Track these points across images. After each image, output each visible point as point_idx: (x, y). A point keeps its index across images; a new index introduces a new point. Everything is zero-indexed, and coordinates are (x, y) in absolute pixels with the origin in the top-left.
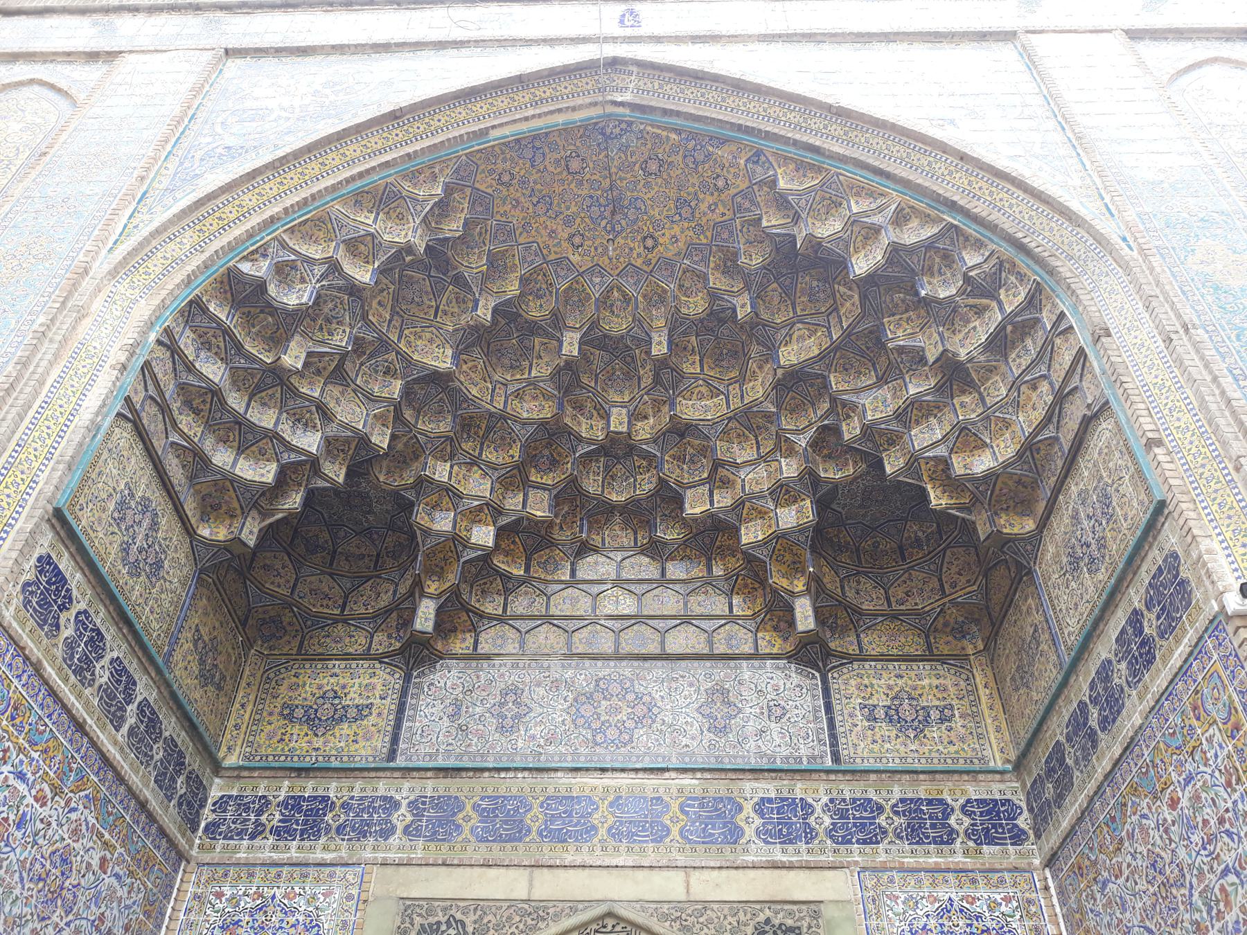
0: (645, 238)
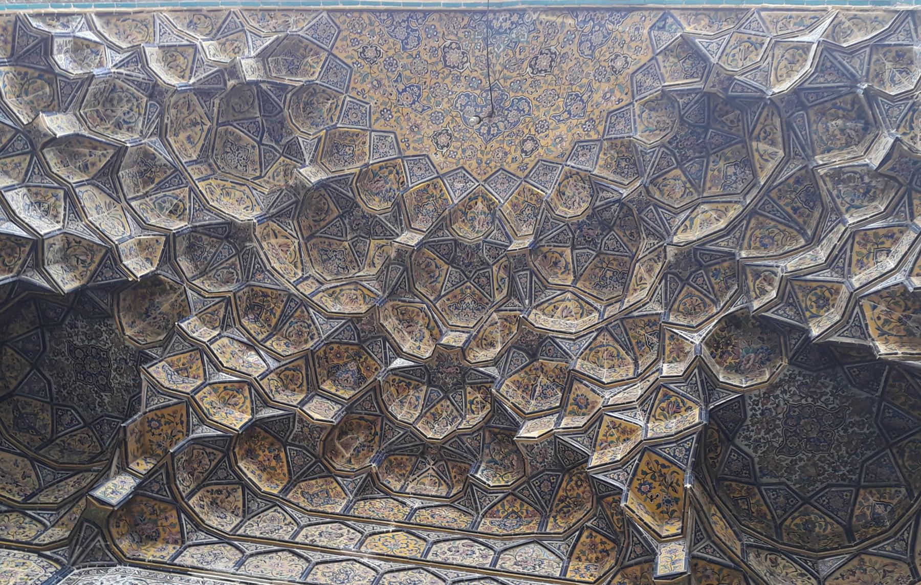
0: (525, 141)
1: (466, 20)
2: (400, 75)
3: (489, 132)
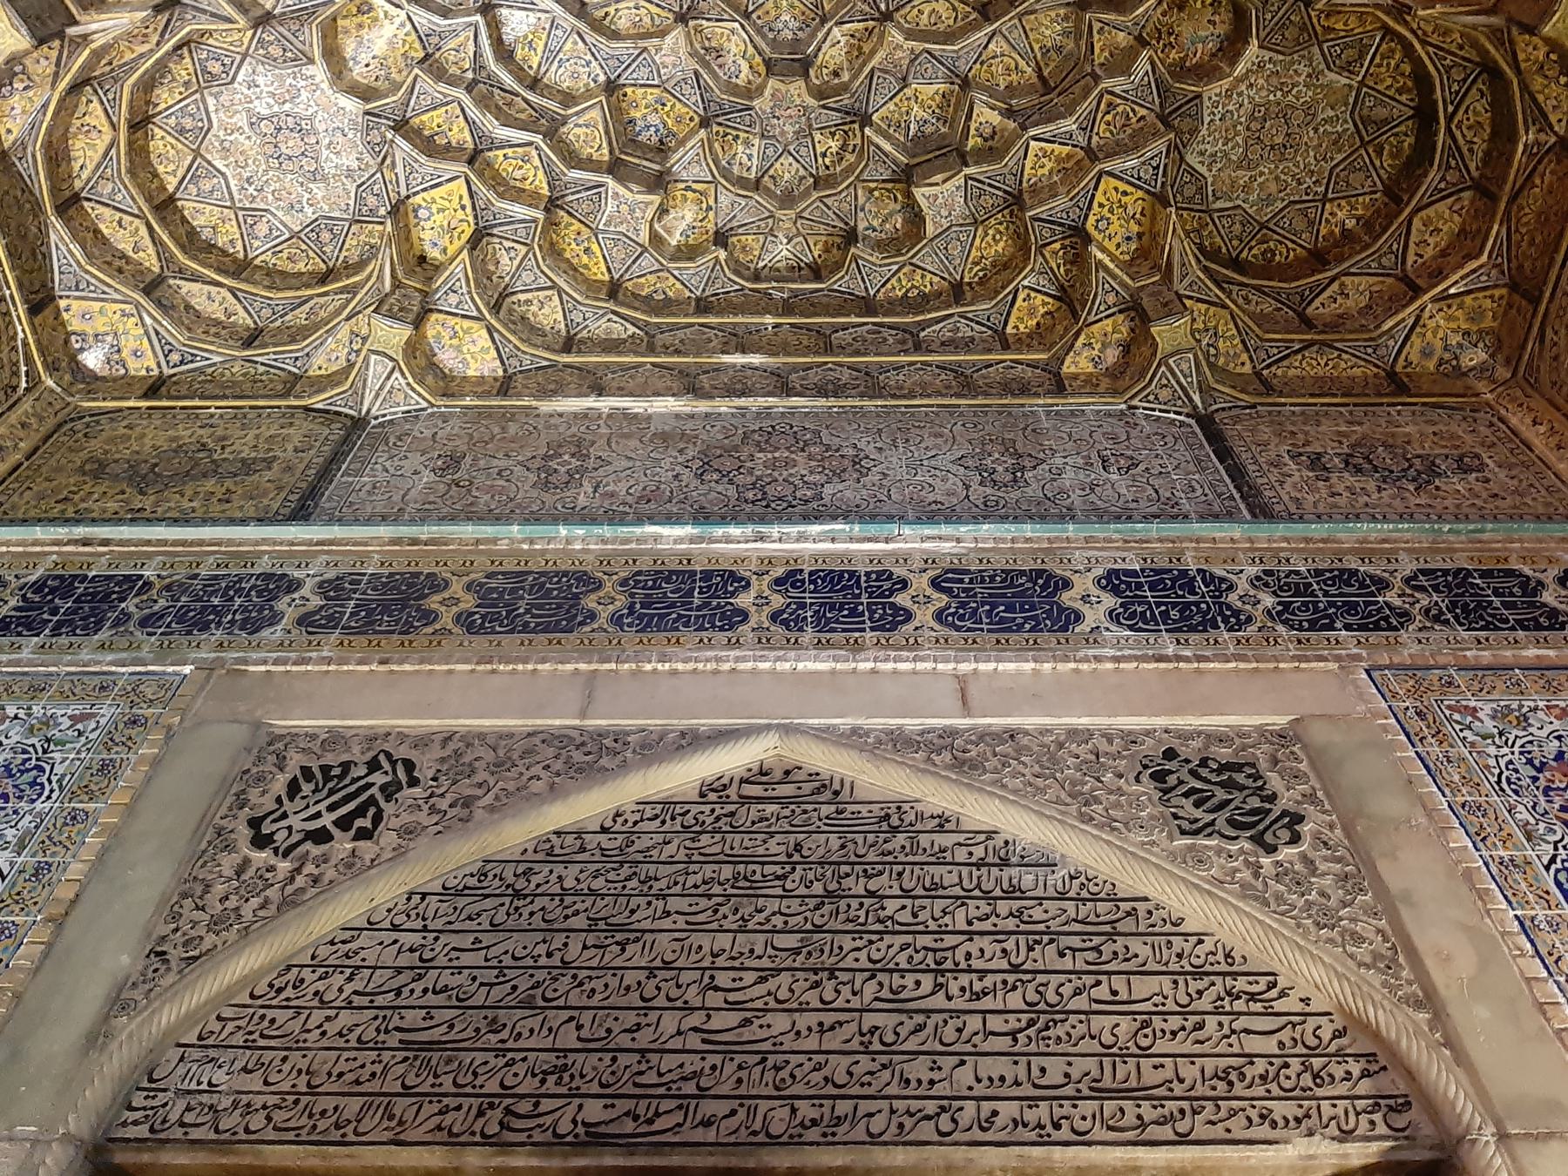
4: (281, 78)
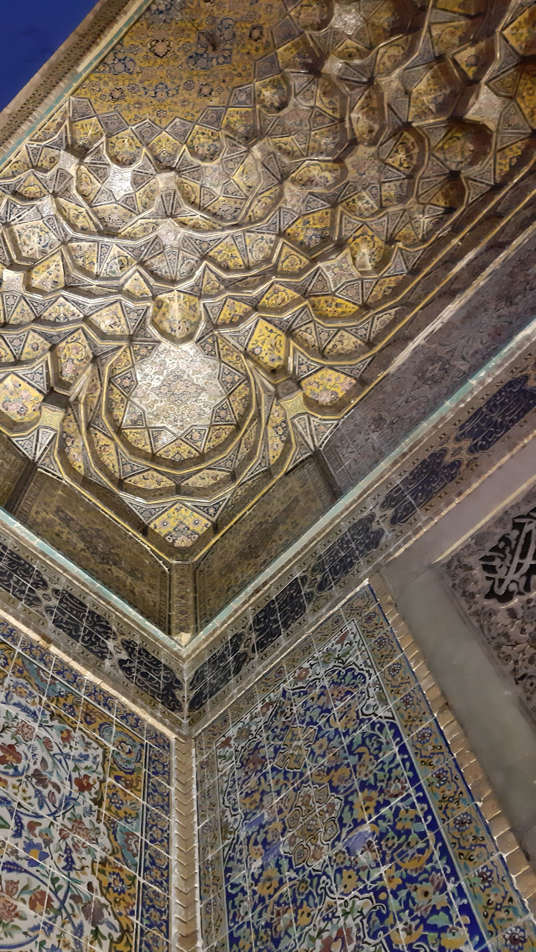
1: (144, 23)
2: (145, 88)
3: (225, 58)
4: (153, 362)
